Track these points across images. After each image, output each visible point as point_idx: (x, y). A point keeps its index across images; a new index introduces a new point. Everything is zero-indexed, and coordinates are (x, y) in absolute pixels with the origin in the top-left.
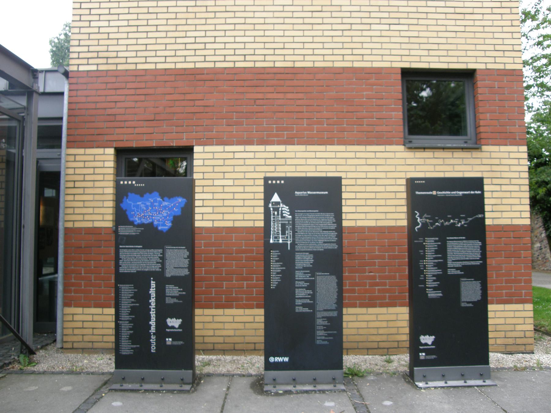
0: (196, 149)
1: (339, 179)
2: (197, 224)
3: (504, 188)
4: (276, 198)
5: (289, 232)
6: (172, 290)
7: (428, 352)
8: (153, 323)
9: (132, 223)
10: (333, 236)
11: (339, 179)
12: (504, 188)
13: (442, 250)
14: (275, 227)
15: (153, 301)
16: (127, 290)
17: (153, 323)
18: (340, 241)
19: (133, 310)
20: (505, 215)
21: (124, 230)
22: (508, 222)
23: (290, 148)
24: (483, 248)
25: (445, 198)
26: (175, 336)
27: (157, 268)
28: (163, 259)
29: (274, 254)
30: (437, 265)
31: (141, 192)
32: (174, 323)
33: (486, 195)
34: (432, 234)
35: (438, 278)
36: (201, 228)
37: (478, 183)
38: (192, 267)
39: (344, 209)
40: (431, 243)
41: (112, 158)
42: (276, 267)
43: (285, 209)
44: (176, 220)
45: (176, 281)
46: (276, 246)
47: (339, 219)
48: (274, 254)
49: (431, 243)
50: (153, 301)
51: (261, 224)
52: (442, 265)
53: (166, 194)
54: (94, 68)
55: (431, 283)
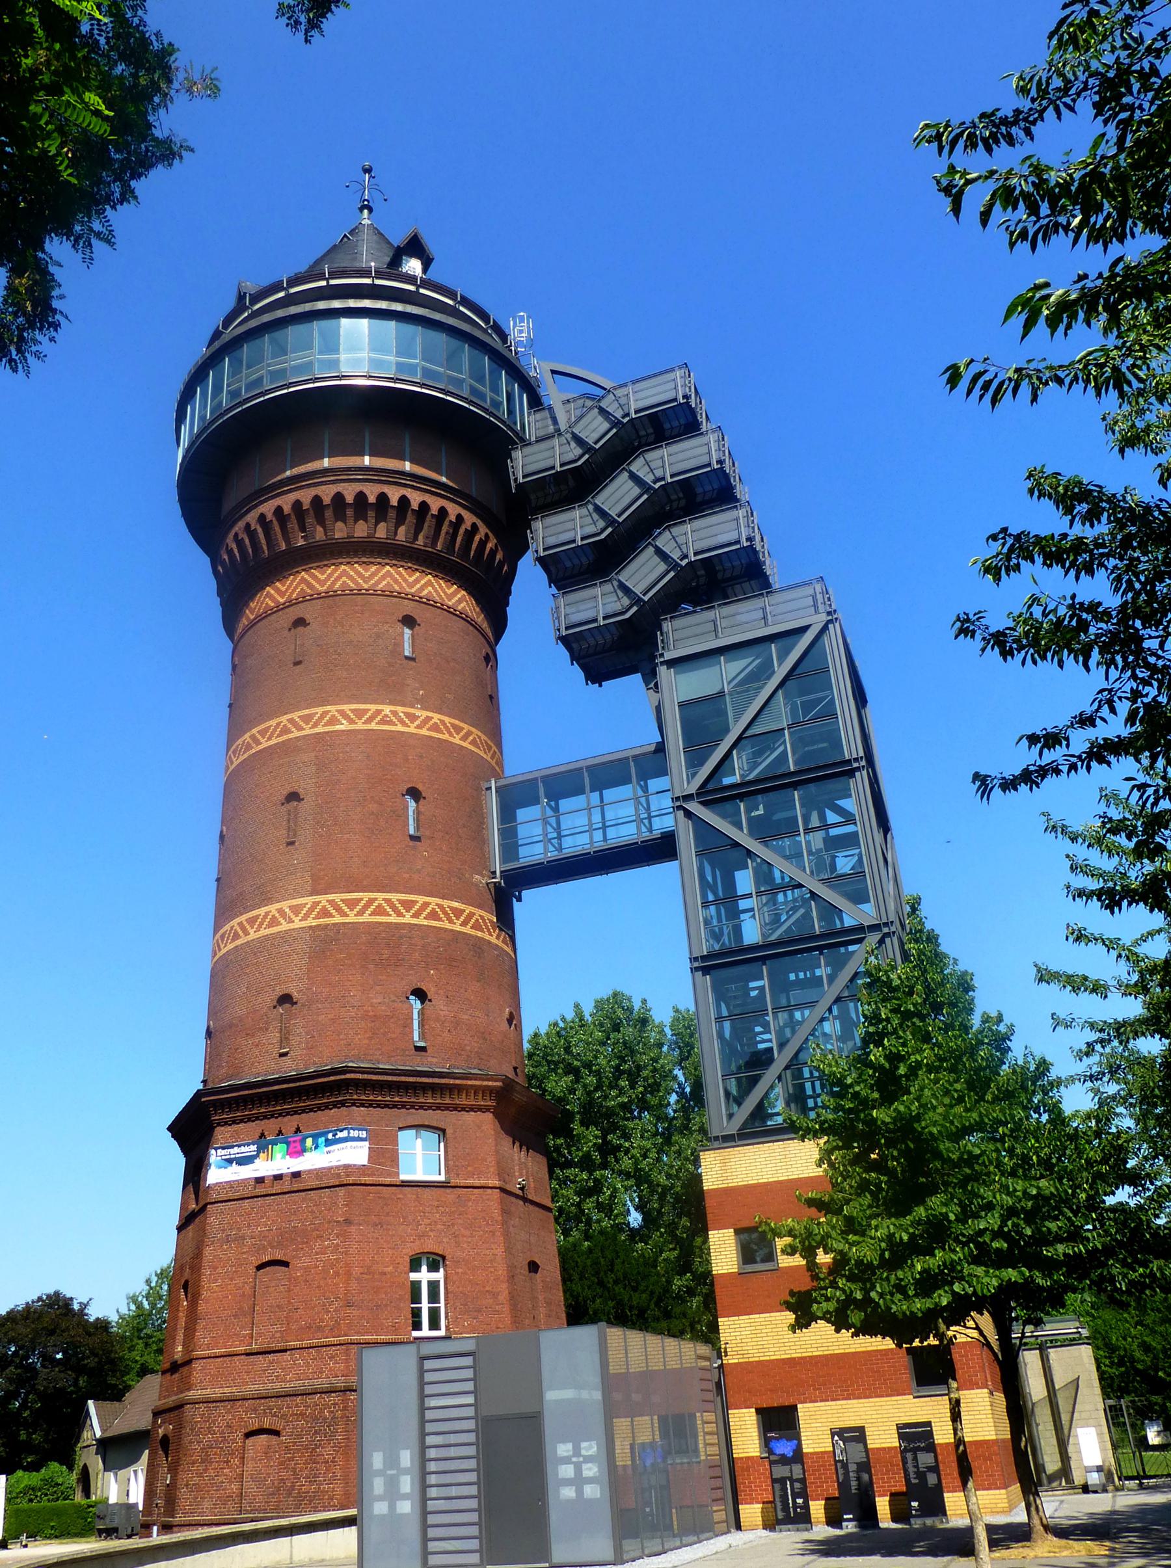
0: (799, 1406)
1: (864, 1427)
2: (804, 1451)
3: (977, 1417)
4: (836, 1438)
5: (844, 1454)
6: (797, 1485)
7: (916, 1510)
8: (790, 1501)
9: (775, 1454)
10: (864, 1454)
11: (864, 1427)
12: (977, 1417)
13: (915, 1459)
14: (838, 1452)
15: (789, 1491)
16: (777, 1486)
17: (790, 1501)
18: (868, 1456)
19: (781, 1496)
20: (980, 1434)
21: (773, 1458)
22: (982, 1438)
23: (849, 1402)
24: (936, 1457)
25: (913, 1432)
26: (801, 1507)
27: (789, 1475)
28: (791, 1470)
29: (839, 1465)
30: (914, 1467)
31: (777, 1439)
32: (800, 1501)
33: (934, 1429)
34: (910, 1451)
35: (915, 1473)
36: (807, 1453)
37: (929, 1424)
38: (804, 1473)
39: (868, 1442)
40: (909, 1456)
41: (754, 1414)
42: (841, 1471)
43: (841, 1443)
44: (795, 1451)
45: (797, 1480)
46: (839, 1461)
47: (865, 1444)
48: (839, 1465)
49: (909, 1456)
50: (789, 1491)
51: (831, 1449)
52: (917, 1467)
53: (789, 1439)
54: (736, 1361)
55: (912, 1475)
